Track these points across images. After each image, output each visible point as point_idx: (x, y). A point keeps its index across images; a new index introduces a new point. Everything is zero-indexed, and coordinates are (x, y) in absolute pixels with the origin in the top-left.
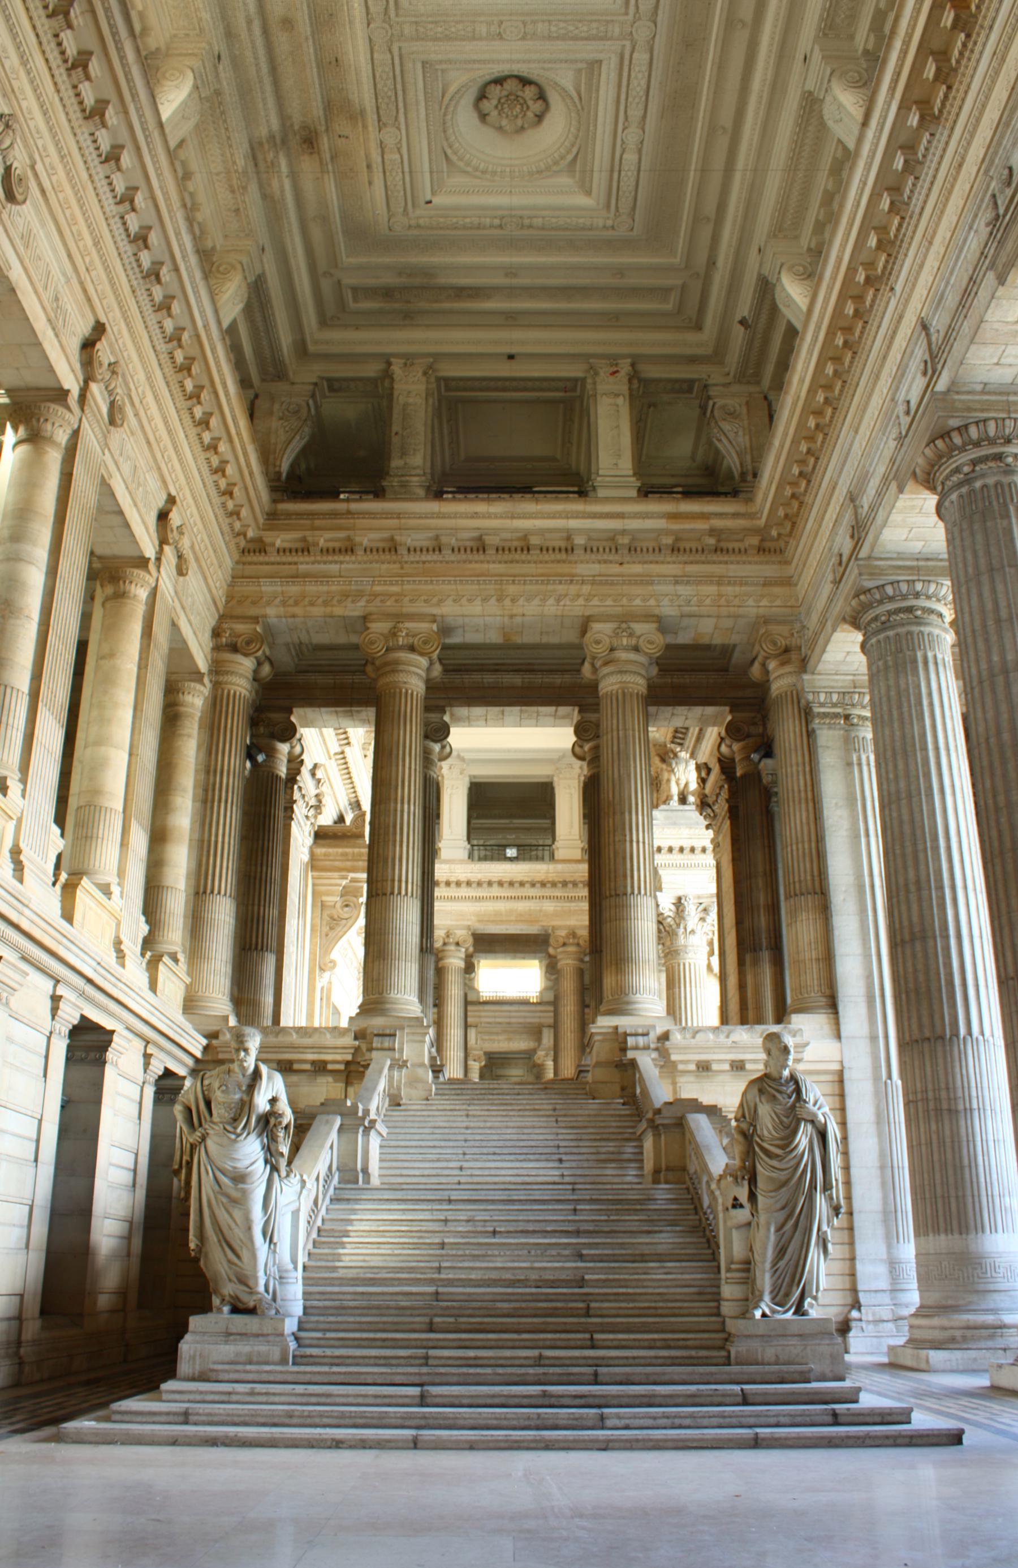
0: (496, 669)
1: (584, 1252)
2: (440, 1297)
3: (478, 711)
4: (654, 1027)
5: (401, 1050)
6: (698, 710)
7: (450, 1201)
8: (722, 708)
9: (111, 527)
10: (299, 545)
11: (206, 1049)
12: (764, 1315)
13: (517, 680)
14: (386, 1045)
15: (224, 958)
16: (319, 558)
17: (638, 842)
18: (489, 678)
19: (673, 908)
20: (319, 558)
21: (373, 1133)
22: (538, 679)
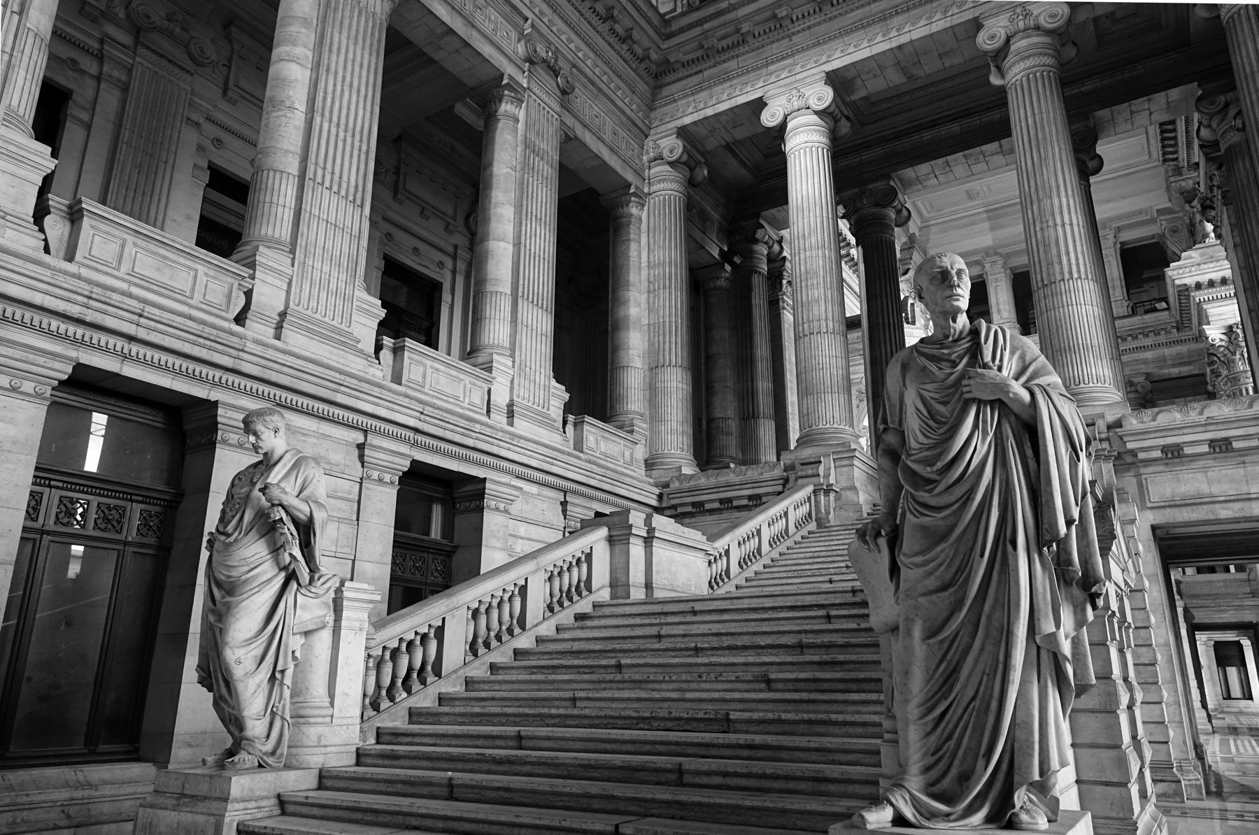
0: (933, 124)
1: (773, 676)
2: (524, 743)
3: (923, 168)
4: (1102, 416)
5: (827, 476)
6: (1160, 98)
7: (694, 613)
8: (1189, 86)
9: (457, 51)
10: (699, 53)
11: (660, 497)
12: (899, 820)
13: (955, 128)
14: (810, 472)
15: (680, 419)
16: (718, 59)
17: (1063, 225)
18: (927, 136)
19: (1224, 337)
20: (718, 59)
21: (655, 543)
22: (976, 121)
